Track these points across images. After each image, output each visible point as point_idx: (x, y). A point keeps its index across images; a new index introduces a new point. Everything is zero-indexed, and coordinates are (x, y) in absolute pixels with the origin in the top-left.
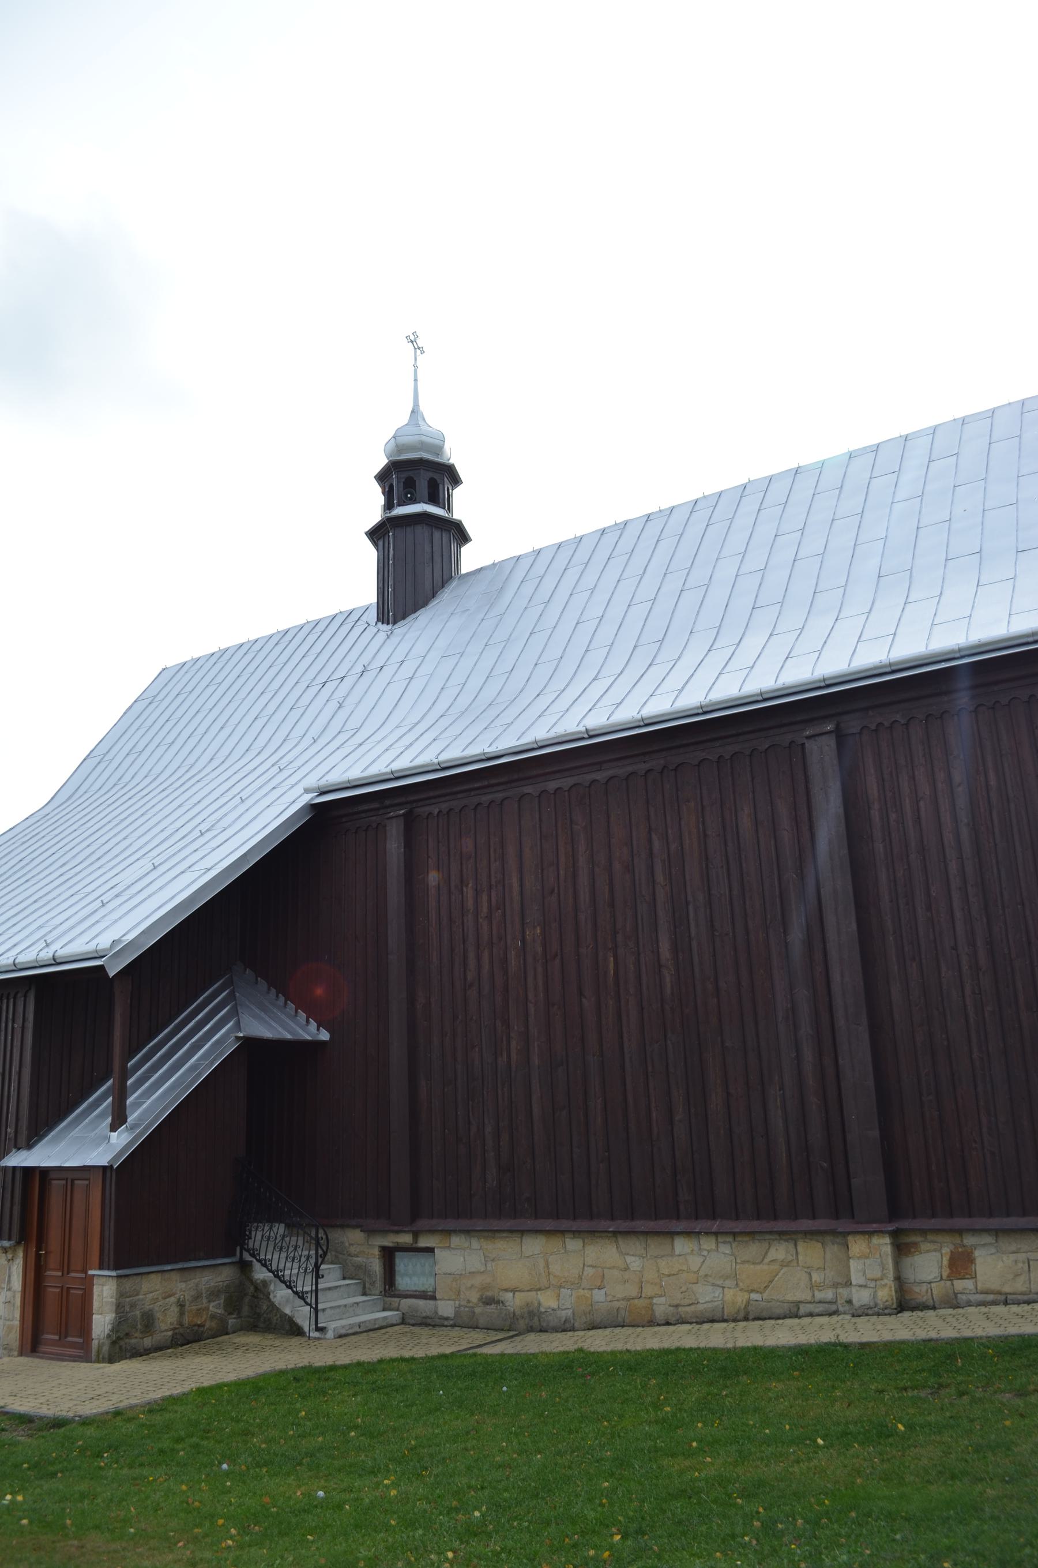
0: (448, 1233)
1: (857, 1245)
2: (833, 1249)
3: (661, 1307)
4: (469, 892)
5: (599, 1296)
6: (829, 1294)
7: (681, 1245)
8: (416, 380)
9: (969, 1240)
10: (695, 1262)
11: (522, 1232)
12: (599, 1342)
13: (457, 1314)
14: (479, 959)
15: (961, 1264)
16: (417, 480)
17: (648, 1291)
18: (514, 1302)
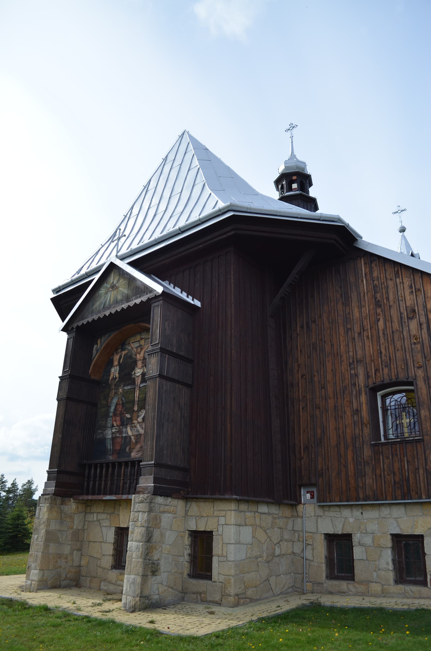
8: (292, 142)
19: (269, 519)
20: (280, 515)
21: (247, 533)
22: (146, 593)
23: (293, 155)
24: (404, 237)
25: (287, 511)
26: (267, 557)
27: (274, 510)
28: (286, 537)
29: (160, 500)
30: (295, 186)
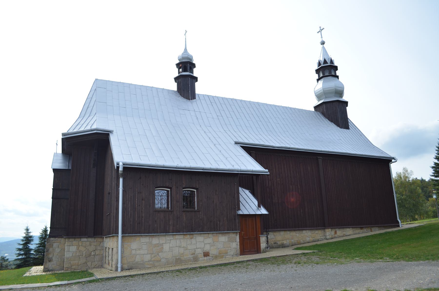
2: (323, 231)
3: (302, 242)
5: (293, 240)
6: (322, 238)
7: (304, 232)
9: (336, 229)
10: (306, 234)
11: (280, 231)
14: (268, 182)
15: (336, 233)
17: (300, 239)
18: (279, 243)
19: (88, 243)
20: (95, 241)
21: (73, 249)
23: (186, 49)
25: (99, 240)
27: (90, 239)
28: (99, 248)
29: (52, 239)
30: (181, 70)
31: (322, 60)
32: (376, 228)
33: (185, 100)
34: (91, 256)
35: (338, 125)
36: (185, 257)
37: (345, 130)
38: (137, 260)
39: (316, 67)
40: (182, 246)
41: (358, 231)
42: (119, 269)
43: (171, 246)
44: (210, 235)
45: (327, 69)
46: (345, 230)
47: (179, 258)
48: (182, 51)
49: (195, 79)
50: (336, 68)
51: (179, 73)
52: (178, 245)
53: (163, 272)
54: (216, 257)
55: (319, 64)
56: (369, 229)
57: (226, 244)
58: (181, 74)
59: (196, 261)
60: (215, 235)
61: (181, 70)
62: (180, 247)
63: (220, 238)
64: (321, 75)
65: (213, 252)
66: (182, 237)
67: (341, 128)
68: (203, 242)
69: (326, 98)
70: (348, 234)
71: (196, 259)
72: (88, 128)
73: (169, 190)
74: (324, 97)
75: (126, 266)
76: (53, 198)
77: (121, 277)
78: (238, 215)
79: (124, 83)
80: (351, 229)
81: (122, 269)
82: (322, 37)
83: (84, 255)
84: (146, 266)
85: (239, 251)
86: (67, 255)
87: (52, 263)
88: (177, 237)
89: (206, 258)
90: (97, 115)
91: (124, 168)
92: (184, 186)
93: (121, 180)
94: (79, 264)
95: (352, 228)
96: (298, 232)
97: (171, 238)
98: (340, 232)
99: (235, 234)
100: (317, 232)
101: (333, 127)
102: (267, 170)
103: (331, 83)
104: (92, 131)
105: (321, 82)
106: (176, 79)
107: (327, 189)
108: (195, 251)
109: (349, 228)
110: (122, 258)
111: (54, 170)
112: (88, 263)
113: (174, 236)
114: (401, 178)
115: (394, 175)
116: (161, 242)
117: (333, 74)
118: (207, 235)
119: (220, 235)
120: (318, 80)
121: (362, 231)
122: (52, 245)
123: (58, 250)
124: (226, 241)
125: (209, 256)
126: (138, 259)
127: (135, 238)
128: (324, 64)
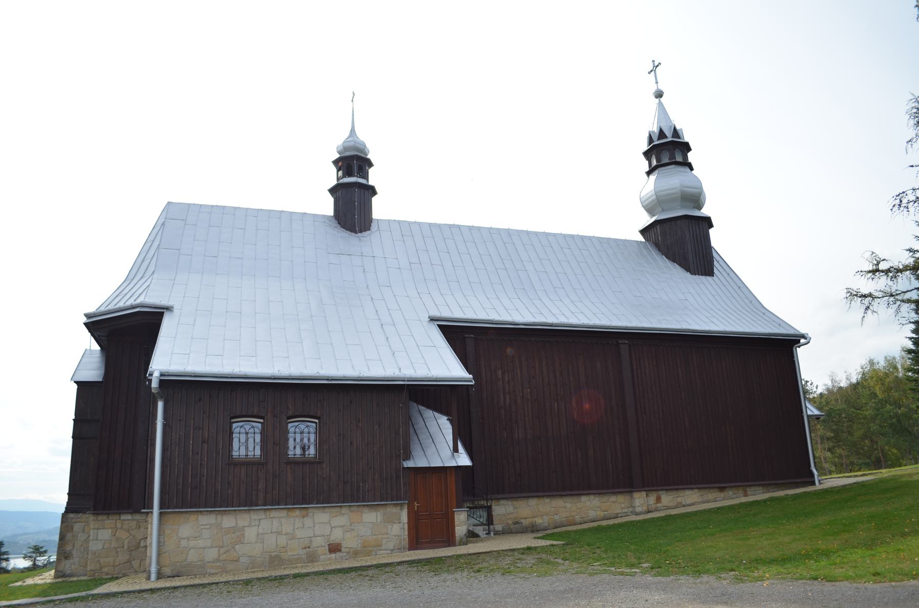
0: (498, 499)
1: (636, 495)
2: (627, 497)
3: (578, 519)
4: (500, 372)
6: (626, 510)
7: (584, 498)
9: (660, 493)
10: (588, 503)
11: (528, 497)
12: (604, 523)
13: (503, 529)
14: (505, 398)
15: (658, 499)
16: (354, 163)
17: (573, 514)
18: (525, 522)
19: (134, 523)
21: (105, 534)
22: (61, 569)
23: (353, 131)
24: (660, 104)
26: (129, 547)
29: (71, 515)
31: (656, 130)
32: (757, 488)
33: (346, 234)
34: (140, 549)
35: (688, 268)
36: (289, 554)
37: (703, 278)
38: (190, 559)
39: (645, 147)
40: (284, 532)
41: (711, 495)
42: (153, 576)
43: (261, 531)
44: (344, 510)
45: (668, 150)
46: (681, 493)
47: (276, 556)
48: (347, 134)
49: (372, 191)
50: (686, 147)
51: (338, 179)
52: (274, 530)
53: (217, 583)
54: (356, 554)
55: (651, 140)
56: (741, 492)
57: (380, 527)
58: (341, 181)
59: (312, 561)
60: (356, 509)
61: (340, 173)
62: (279, 533)
63: (364, 516)
64: (654, 163)
65: (350, 542)
66: (284, 513)
67: (693, 273)
68: (329, 522)
69: (663, 210)
70: (689, 501)
71: (312, 558)
72: (131, 302)
73: (262, 421)
74: (660, 209)
75: (167, 571)
76: (75, 437)
77: (134, 592)
78: (404, 468)
79: (224, 207)
80: (696, 491)
81: (160, 576)
82: (657, 83)
83: (126, 547)
84: (209, 571)
85: (406, 543)
86: (95, 546)
87: (71, 561)
88: (274, 514)
89: (333, 555)
90: (155, 276)
91: (162, 383)
92: (290, 413)
93: (160, 405)
94: (117, 564)
95: (699, 488)
96: (568, 499)
97: (261, 515)
98: (667, 499)
99: (399, 508)
100: (613, 498)
101: (676, 272)
102: (471, 376)
103: (674, 179)
104: (134, 308)
105: (653, 177)
106: (332, 191)
107: (643, 403)
108: (311, 541)
109: (692, 489)
110: (159, 554)
111: (80, 384)
112: (133, 562)
113: (268, 513)
114: (896, 368)
115: (429, 414)
116: (241, 523)
117: (679, 158)
118: (338, 509)
119: (366, 510)
120: (649, 173)
121: (722, 495)
122: (72, 528)
123: (82, 537)
124: (379, 520)
125: (340, 550)
126: (192, 556)
127: (187, 516)
128: (658, 139)
